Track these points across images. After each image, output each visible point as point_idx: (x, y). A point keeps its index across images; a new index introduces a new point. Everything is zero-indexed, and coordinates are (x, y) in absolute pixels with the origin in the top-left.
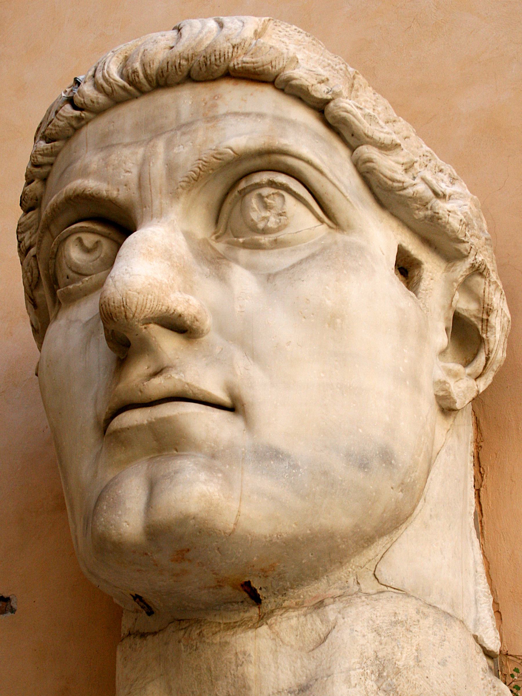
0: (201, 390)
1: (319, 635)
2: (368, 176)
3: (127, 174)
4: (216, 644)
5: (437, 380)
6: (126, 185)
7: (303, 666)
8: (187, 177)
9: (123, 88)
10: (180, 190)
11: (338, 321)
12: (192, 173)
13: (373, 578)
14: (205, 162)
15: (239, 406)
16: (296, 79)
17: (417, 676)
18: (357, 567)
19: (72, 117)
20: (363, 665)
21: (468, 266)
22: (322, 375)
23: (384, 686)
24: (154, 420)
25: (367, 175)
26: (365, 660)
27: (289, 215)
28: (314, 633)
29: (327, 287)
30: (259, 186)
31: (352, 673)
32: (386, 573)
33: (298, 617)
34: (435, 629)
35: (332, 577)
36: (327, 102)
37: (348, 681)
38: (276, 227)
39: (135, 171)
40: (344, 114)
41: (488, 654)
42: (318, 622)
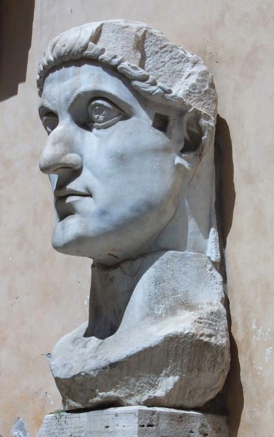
15: (93, 196)
16: (104, 59)
17: (172, 281)
25: (136, 92)
34: (181, 261)
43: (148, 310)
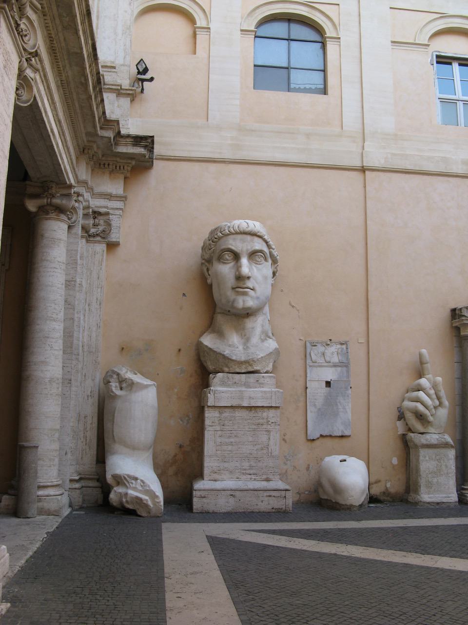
25: (270, 253)
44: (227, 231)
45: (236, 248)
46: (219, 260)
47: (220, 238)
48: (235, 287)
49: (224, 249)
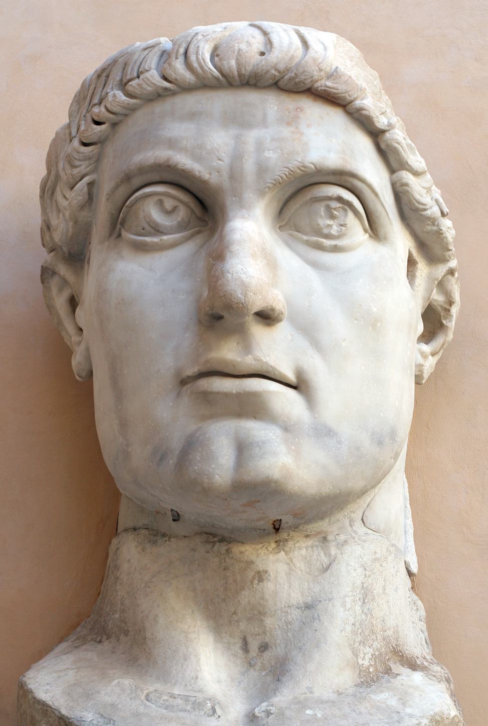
0: (280, 373)
1: (322, 565)
2: (401, 195)
3: (220, 162)
4: (242, 562)
5: (418, 363)
6: (218, 172)
7: (309, 588)
8: (274, 180)
9: (217, 79)
10: (267, 190)
11: (379, 324)
12: (280, 178)
13: (361, 522)
14: (292, 171)
16: (366, 110)
18: (351, 512)
19: (162, 87)
20: (355, 594)
21: (447, 269)
22: (363, 368)
23: (365, 610)
24: (242, 392)
25: (400, 195)
26: (355, 589)
27: (348, 226)
28: (318, 562)
29: (374, 296)
30: (330, 198)
31: (347, 599)
32: (370, 518)
33: (307, 548)
35: (333, 518)
36: (383, 132)
37: (344, 605)
38: (337, 234)
39: (227, 160)
40: (396, 145)
41: (410, 574)
42: (322, 555)
43: (349, 654)
44: (154, 76)
45: (198, 158)
46: (120, 235)
47: (117, 120)
48: (190, 371)
49: (142, 170)
